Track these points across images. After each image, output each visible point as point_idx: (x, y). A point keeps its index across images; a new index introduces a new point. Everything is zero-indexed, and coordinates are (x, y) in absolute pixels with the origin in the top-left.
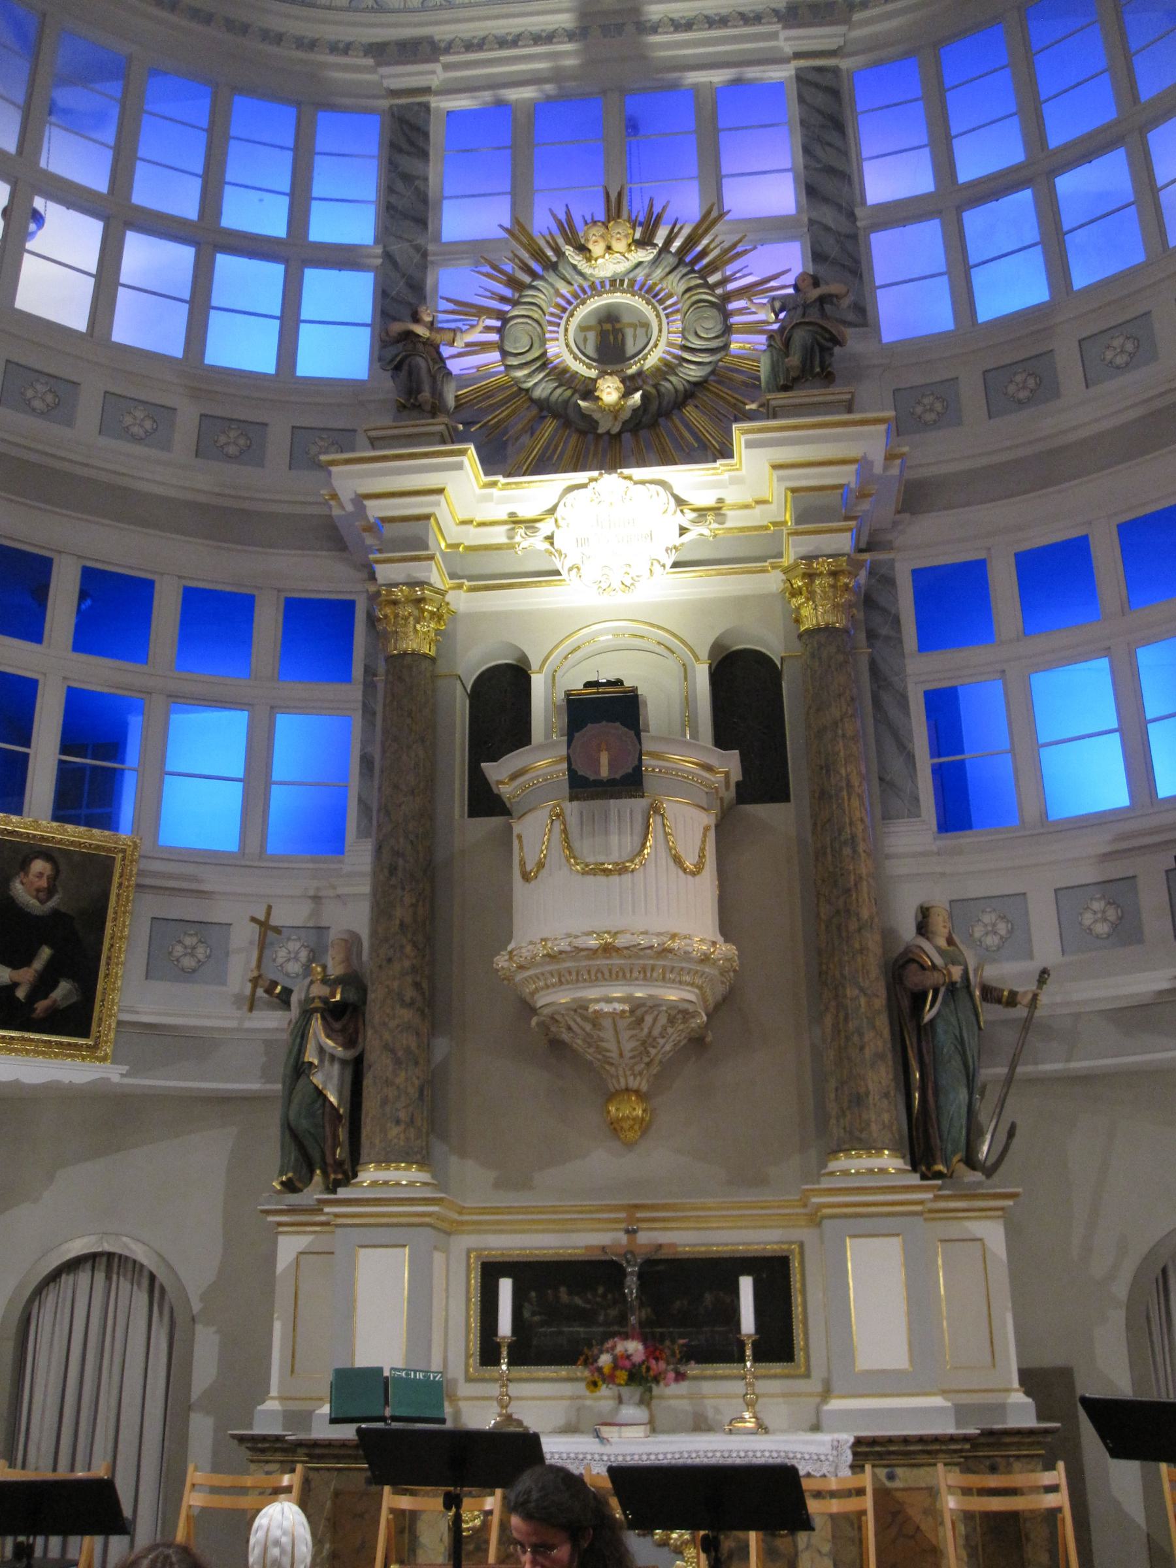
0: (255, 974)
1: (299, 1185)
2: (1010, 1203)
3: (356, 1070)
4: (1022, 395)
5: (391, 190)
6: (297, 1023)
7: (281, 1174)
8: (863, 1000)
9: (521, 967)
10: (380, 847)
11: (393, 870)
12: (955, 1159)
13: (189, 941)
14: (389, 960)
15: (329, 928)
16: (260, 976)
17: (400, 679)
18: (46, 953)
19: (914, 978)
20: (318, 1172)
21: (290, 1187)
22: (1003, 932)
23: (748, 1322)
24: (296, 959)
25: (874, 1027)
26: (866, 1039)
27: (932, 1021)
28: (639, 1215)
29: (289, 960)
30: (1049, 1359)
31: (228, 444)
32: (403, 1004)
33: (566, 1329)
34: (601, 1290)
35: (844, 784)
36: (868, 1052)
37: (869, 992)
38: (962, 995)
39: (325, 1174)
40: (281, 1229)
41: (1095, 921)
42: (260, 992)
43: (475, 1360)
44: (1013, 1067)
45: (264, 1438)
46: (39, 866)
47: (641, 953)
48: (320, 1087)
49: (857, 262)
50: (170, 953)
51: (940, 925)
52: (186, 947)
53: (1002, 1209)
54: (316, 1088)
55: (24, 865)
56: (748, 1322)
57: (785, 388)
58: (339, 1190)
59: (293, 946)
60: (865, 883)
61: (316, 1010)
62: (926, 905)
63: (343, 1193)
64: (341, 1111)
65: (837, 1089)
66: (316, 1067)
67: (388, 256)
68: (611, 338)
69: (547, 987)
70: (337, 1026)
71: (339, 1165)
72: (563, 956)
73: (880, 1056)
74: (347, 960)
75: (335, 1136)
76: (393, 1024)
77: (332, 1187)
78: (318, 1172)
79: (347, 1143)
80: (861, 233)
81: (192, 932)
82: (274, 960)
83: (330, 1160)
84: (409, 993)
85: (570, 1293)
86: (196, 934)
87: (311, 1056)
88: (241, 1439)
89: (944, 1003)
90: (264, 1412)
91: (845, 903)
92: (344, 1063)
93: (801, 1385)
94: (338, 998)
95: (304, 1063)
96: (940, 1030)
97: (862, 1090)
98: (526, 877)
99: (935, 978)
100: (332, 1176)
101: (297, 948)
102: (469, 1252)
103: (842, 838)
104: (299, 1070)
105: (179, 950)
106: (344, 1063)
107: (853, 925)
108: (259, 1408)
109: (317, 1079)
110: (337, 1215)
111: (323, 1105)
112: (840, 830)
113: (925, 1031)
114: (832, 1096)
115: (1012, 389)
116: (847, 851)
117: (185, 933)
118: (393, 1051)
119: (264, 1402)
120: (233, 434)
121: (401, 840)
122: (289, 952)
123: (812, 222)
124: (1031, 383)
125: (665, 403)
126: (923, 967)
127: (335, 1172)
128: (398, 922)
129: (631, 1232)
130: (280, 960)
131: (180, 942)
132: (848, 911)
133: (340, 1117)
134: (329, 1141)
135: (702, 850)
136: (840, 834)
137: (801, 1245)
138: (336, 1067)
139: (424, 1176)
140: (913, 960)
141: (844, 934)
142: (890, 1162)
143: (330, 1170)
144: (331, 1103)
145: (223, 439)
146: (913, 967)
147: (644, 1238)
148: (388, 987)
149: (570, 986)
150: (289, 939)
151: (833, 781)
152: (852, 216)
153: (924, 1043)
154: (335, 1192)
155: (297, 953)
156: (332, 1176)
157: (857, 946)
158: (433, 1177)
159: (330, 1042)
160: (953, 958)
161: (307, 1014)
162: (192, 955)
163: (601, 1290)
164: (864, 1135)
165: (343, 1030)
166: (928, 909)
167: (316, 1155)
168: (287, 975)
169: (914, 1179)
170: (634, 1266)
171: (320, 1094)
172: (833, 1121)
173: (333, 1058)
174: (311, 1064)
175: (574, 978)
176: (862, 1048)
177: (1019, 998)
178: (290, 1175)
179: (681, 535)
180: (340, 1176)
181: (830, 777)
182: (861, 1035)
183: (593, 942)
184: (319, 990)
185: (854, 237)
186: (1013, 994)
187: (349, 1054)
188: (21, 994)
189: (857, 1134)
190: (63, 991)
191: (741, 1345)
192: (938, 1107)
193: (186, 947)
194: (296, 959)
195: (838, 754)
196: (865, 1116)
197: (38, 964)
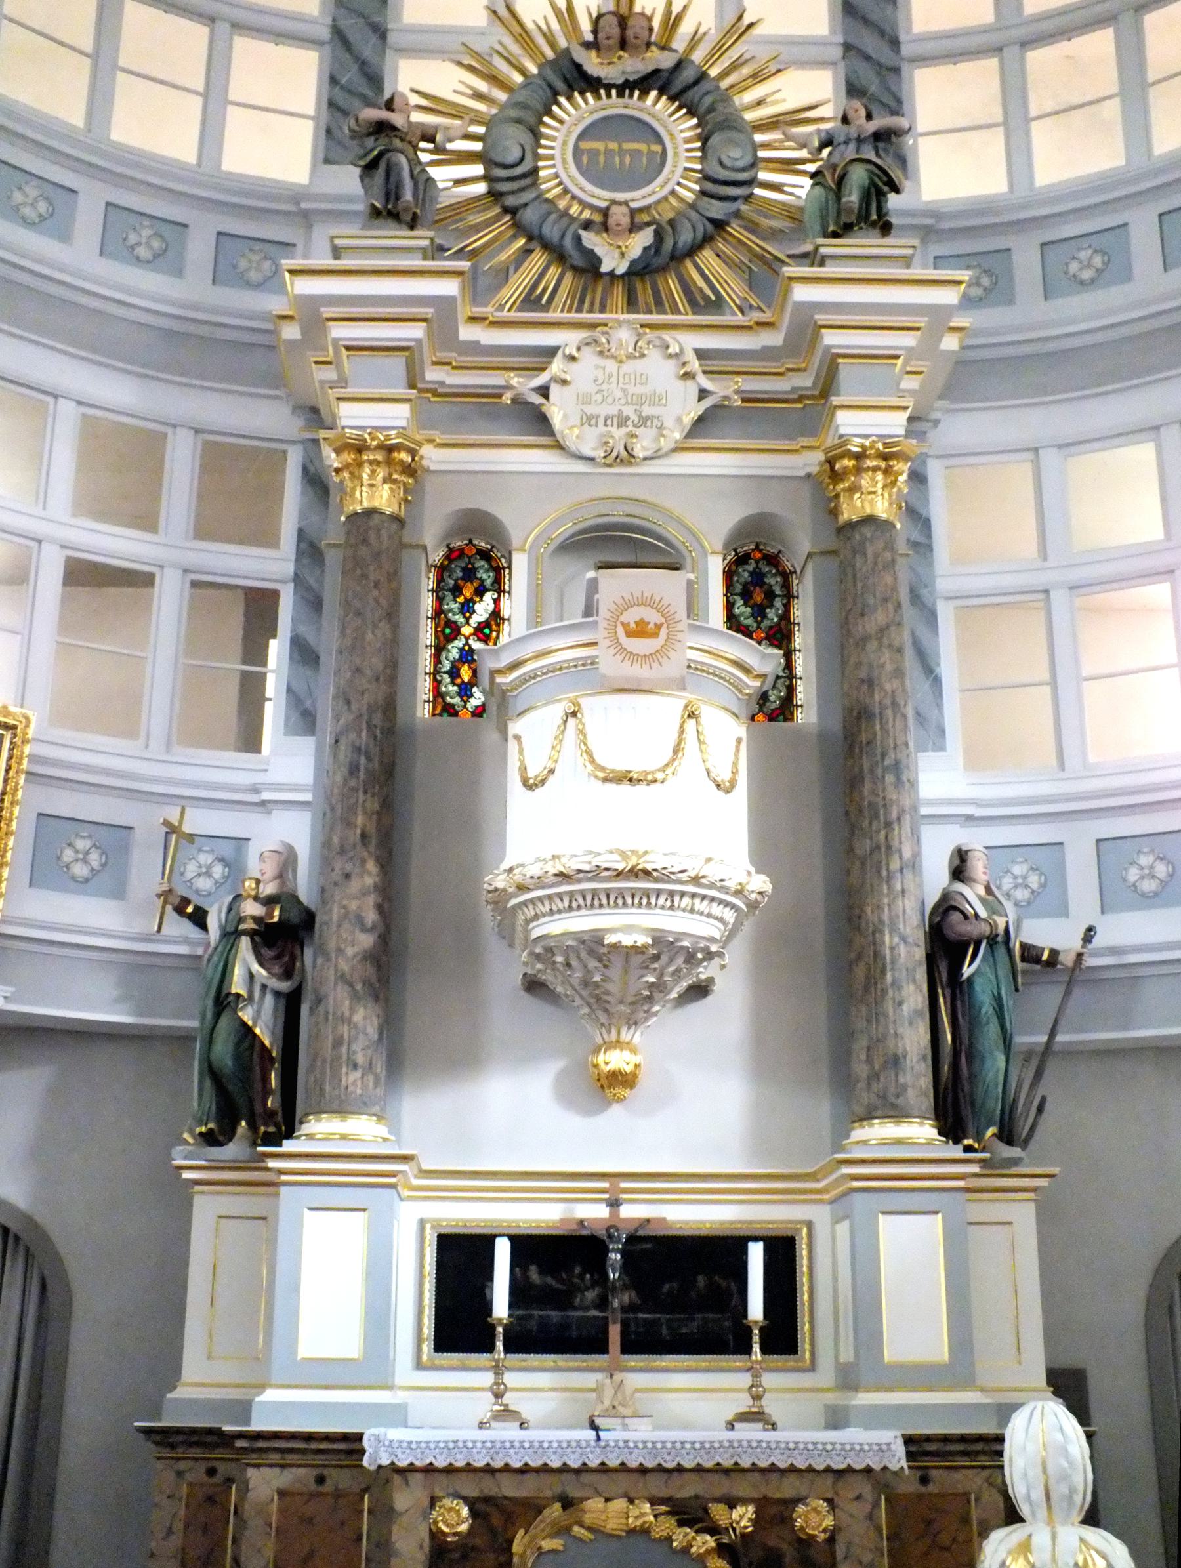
0: (165, 887)
1: (221, 1138)
2: (1043, 1182)
3: (291, 1004)
4: (1087, 275)
6: (216, 948)
7: (201, 1122)
8: (902, 949)
9: (522, 888)
10: (337, 741)
11: (353, 770)
12: (992, 1130)
13: (81, 844)
14: (347, 876)
15: (248, 840)
16: (170, 891)
17: (365, 541)
19: (957, 926)
20: (243, 1123)
21: (210, 1139)
22: (1035, 886)
23: (756, 1309)
24: (208, 874)
25: (914, 981)
26: (905, 993)
27: (970, 979)
28: (623, 1185)
29: (199, 875)
30: (1068, 1360)
31: (139, 244)
32: (364, 929)
33: (536, 1313)
34: (578, 1270)
35: (888, 701)
36: (907, 1008)
37: (910, 940)
38: (1001, 952)
39: (253, 1126)
40: (197, 1188)
41: (1142, 878)
42: (169, 908)
43: (427, 1347)
44: (1052, 1034)
45: (179, 1431)
47: (673, 877)
48: (250, 1023)
49: (899, 101)
50: (59, 858)
52: (77, 852)
53: (1034, 1190)
54: (245, 1024)
56: (756, 1309)
57: (835, 235)
58: (285, 1142)
59: (205, 858)
60: (908, 817)
61: (244, 932)
62: (964, 848)
63: (288, 1146)
64: (274, 1054)
65: (869, 1049)
66: (245, 1000)
67: (339, 34)
68: (617, 160)
69: (551, 912)
70: (268, 953)
71: (270, 1115)
72: (581, 875)
73: (918, 1013)
74: (280, 876)
75: (265, 1080)
76: (350, 951)
77: (274, 1139)
78: (243, 1123)
79: (278, 1093)
80: (905, 68)
81: (85, 834)
82: (182, 874)
83: (258, 1109)
84: (371, 916)
85: (541, 1272)
86: (90, 837)
87: (238, 985)
88: (148, 1432)
89: (984, 959)
90: (171, 1400)
91: (887, 837)
92: (277, 994)
93: (806, 1380)
94: (276, 919)
95: (229, 994)
96: (977, 988)
97: (900, 1051)
98: (528, 785)
99: (985, 929)
100: (262, 1129)
101: (209, 862)
102: (422, 1223)
103: (886, 763)
104: (223, 1002)
105: (68, 855)
106: (277, 994)
107: (895, 865)
108: (169, 1396)
109: (246, 1015)
110: (281, 1172)
111: (252, 1047)
112: (884, 755)
113: (959, 988)
114: (863, 1057)
115: (1074, 267)
116: (890, 778)
117: (78, 836)
118: (351, 985)
119: (175, 1388)
120: (146, 233)
121: (364, 734)
122: (200, 867)
123: (848, 47)
124: (1098, 261)
125: (680, 244)
126: (966, 917)
127: (266, 1125)
128: (358, 831)
130: (189, 875)
131: (70, 845)
132: (889, 847)
133: (272, 1060)
134: (258, 1086)
135: (735, 764)
136: (883, 759)
137: (809, 1225)
138: (269, 999)
139: (382, 1130)
140: (955, 908)
141: (884, 873)
142: (923, 1131)
143: (259, 1121)
144: (263, 1044)
145: (133, 238)
146: (955, 917)
147: (631, 1212)
148: (344, 907)
149: (583, 912)
150: (200, 850)
151: (877, 697)
153: (959, 1002)
154: (280, 1145)
155: (209, 867)
156: (262, 1129)
157: (898, 887)
158: (390, 1132)
159: (263, 972)
160: (995, 907)
161: (231, 935)
162: (85, 861)
163: (578, 1270)
164: (900, 1101)
165: (277, 957)
166: (966, 852)
167: (241, 1101)
168: (197, 892)
169: (956, 1152)
170: (619, 1242)
171: (246, 1031)
172: (861, 1085)
173: (264, 987)
174: (238, 995)
175: (589, 902)
176: (900, 1004)
177: (1061, 958)
178: (211, 1125)
179: (700, 399)
180: (272, 1129)
181: (873, 692)
182: (900, 988)
184: (251, 909)
185: (896, 71)
186: (1054, 953)
187: (285, 986)
189: (893, 1100)
191: (748, 1330)
192: (972, 1077)
193: (77, 852)
194: (208, 874)
195: (883, 666)
196: (902, 1080)
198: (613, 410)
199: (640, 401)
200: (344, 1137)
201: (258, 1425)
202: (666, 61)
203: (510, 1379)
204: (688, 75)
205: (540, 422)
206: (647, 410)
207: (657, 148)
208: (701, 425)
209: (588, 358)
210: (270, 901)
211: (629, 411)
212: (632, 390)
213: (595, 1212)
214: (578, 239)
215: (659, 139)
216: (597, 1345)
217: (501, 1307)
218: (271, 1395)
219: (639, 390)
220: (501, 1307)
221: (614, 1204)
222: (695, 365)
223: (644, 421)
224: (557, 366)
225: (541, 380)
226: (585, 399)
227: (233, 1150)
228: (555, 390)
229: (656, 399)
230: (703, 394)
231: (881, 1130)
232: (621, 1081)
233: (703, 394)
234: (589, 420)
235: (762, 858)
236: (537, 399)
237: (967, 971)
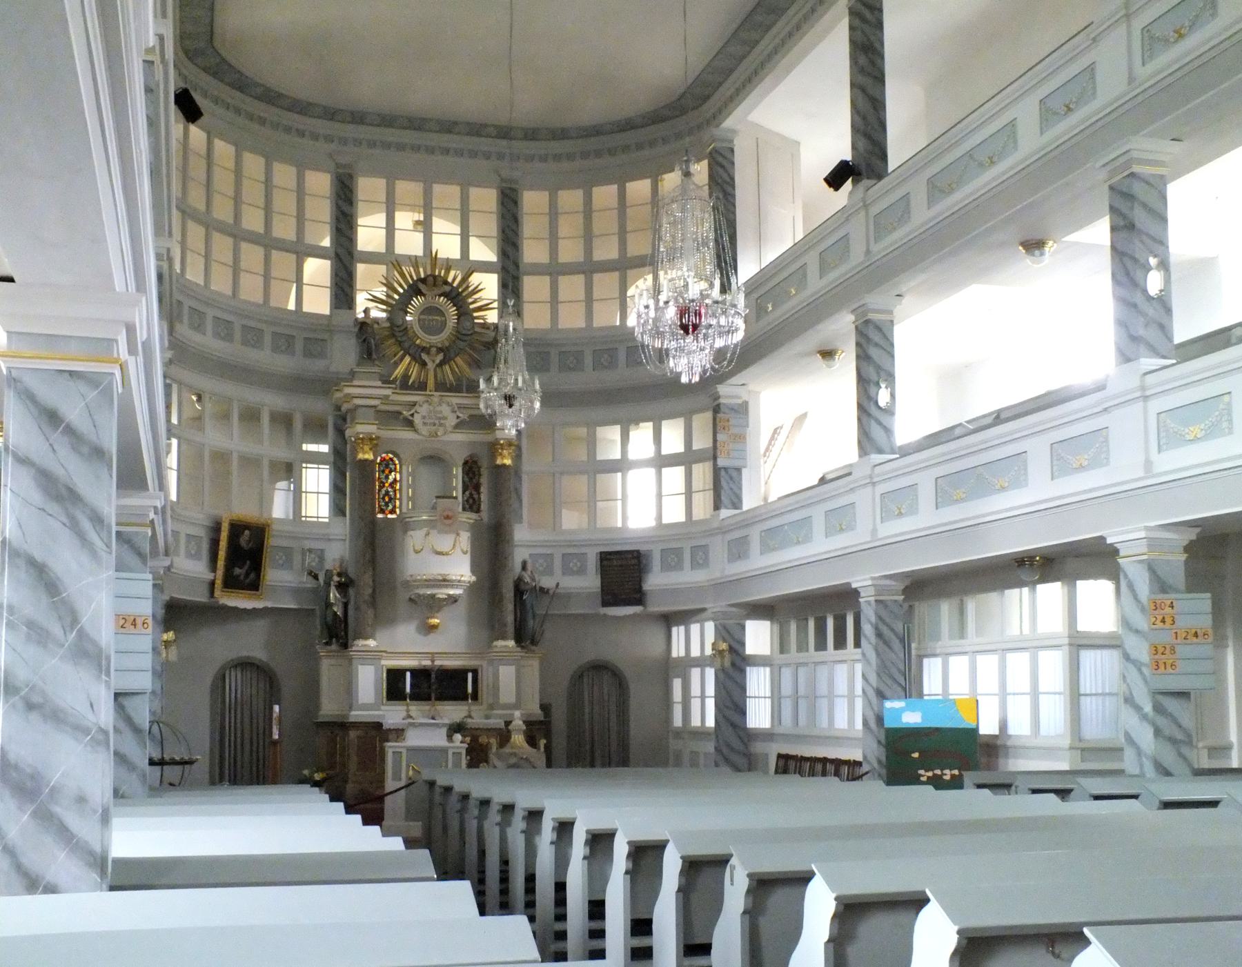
3: (346, 605)
5: (338, 219)
18: (248, 562)
19: (523, 587)
46: (247, 532)
51: (529, 567)
55: (243, 533)
67: (337, 255)
84: (371, 583)
93: (481, 707)
104: (328, 605)
129: (433, 661)
137: (482, 666)
142: (511, 643)
152: (517, 266)
160: (533, 580)
183: (441, 578)
187: (344, 600)
188: (242, 577)
190: (252, 576)
197: (246, 567)
198: (432, 421)
199: (440, 418)
200: (365, 645)
201: (352, 720)
202: (447, 288)
203: (410, 708)
204: (454, 294)
205: (409, 423)
206: (442, 422)
207: (443, 319)
208: (457, 426)
209: (426, 406)
210: (339, 575)
211: (437, 422)
212: (438, 415)
213: (427, 663)
214: (420, 355)
215: (443, 315)
216: (428, 698)
217: (408, 689)
218: (353, 713)
219: (440, 415)
220: (408, 689)
221: (433, 661)
222: (456, 409)
223: (441, 425)
224: (417, 407)
225: (411, 412)
226: (424, 417)
227: (334, 647)
228: (416, 415)
229: (445, 418)
230: (458, 417)
231: (500, 643)
232: (434, 628)
233: (458, 417)
234: (425, 424)
235: (473, 571)
236: (411, 418)
237: (524, 597)
